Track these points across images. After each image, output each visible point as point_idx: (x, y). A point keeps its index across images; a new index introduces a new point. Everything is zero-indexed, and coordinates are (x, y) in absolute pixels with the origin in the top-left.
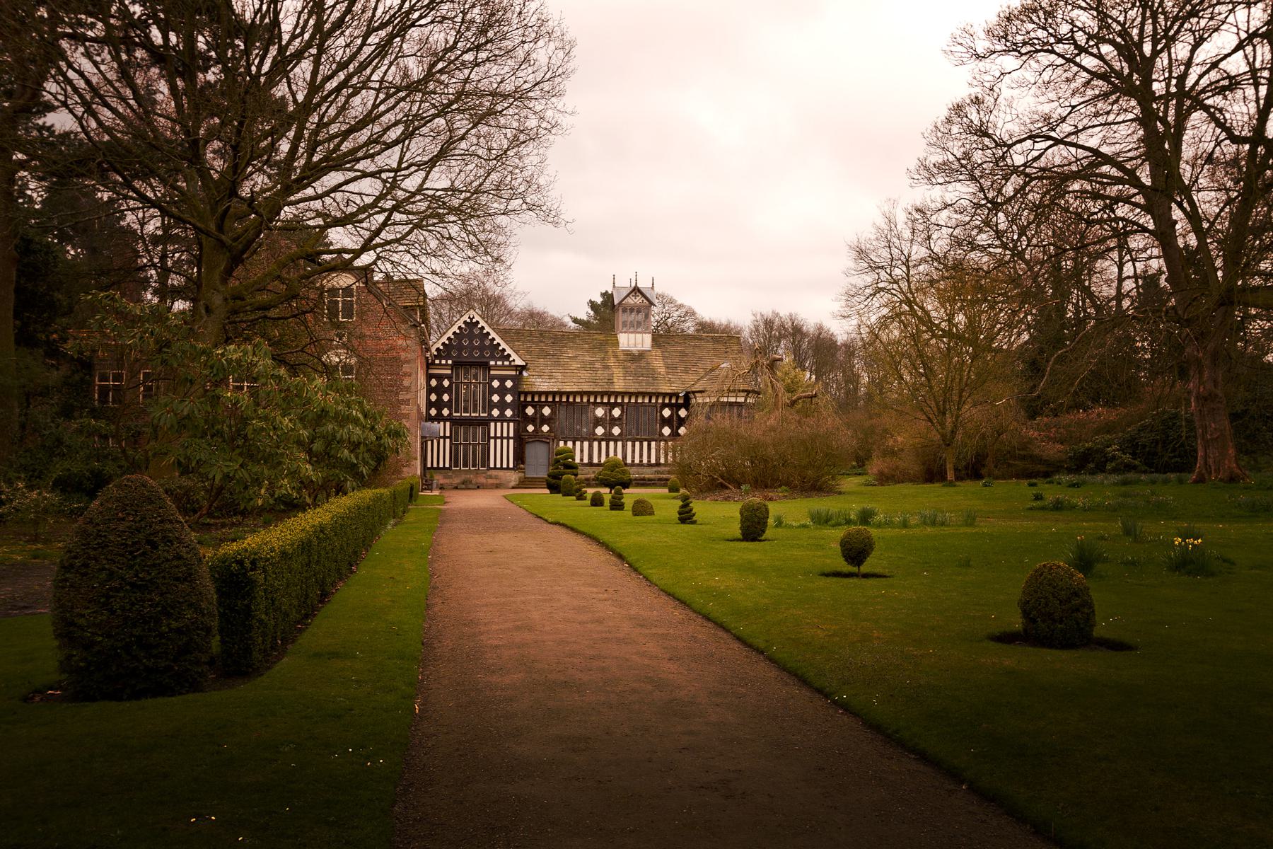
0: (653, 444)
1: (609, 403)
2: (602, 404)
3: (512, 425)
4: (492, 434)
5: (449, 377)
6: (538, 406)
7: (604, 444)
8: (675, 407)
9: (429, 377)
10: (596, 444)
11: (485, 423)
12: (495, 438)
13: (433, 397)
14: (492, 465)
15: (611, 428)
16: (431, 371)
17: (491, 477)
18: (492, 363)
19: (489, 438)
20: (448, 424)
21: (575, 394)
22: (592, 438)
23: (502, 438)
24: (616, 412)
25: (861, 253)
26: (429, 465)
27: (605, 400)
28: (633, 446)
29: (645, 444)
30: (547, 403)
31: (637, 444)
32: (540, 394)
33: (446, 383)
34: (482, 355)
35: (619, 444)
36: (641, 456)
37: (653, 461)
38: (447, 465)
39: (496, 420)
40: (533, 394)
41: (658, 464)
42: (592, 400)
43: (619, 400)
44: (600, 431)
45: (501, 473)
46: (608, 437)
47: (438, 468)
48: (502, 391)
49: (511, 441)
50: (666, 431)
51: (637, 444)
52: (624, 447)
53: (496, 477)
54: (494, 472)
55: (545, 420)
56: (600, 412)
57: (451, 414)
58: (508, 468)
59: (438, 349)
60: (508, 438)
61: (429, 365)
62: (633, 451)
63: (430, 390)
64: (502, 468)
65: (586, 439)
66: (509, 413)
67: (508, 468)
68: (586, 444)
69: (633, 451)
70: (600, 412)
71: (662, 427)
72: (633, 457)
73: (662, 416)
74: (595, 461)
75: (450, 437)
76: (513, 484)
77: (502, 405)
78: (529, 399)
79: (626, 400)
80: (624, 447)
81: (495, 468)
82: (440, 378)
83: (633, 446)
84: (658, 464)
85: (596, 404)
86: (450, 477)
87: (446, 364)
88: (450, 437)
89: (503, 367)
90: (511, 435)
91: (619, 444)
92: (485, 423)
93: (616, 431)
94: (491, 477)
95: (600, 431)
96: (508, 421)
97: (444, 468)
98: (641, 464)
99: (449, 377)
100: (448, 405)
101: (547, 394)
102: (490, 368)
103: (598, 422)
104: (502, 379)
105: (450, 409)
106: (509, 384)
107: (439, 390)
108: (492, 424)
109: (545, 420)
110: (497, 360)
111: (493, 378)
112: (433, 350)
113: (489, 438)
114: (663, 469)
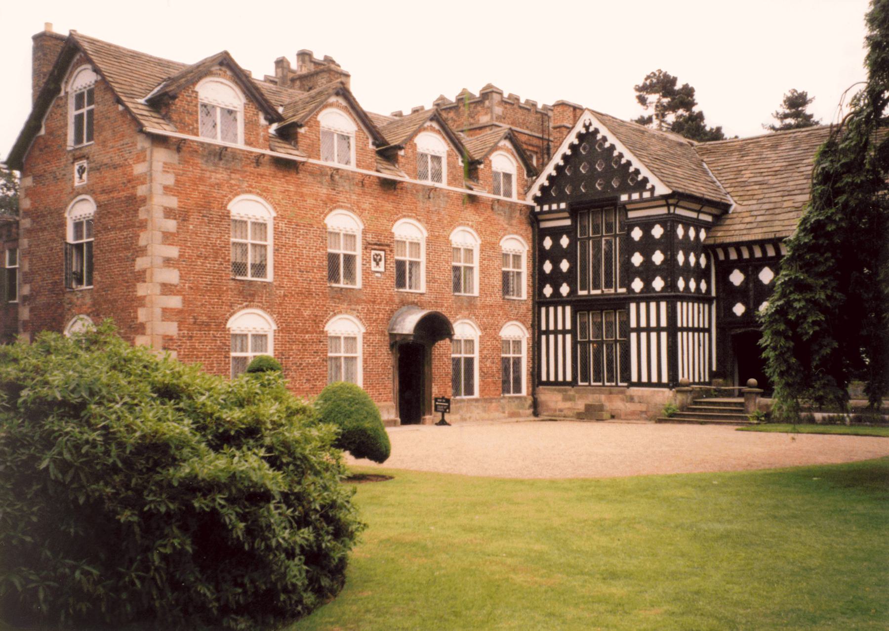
4: (633, 324)
5: (568, 231)
11: (620, 304)
13: (548, 267)
14: (634, 378)
17: (631, 399)
18: (624, 198)
20: (568, 309)
23: (648, 330)
38: (569, 378)
39: (638, 299)
47: (556, 383)
54: (634, 391)
57: (573, 292)
58: (659, 384)
60: (659, 329)
64: (649, 384)
82: (556, 234)
87: (559, 211)
96: (658, 299)
100: (570, 277)
102: (624, 209)
104: (647, 225)
108: (633, 306)
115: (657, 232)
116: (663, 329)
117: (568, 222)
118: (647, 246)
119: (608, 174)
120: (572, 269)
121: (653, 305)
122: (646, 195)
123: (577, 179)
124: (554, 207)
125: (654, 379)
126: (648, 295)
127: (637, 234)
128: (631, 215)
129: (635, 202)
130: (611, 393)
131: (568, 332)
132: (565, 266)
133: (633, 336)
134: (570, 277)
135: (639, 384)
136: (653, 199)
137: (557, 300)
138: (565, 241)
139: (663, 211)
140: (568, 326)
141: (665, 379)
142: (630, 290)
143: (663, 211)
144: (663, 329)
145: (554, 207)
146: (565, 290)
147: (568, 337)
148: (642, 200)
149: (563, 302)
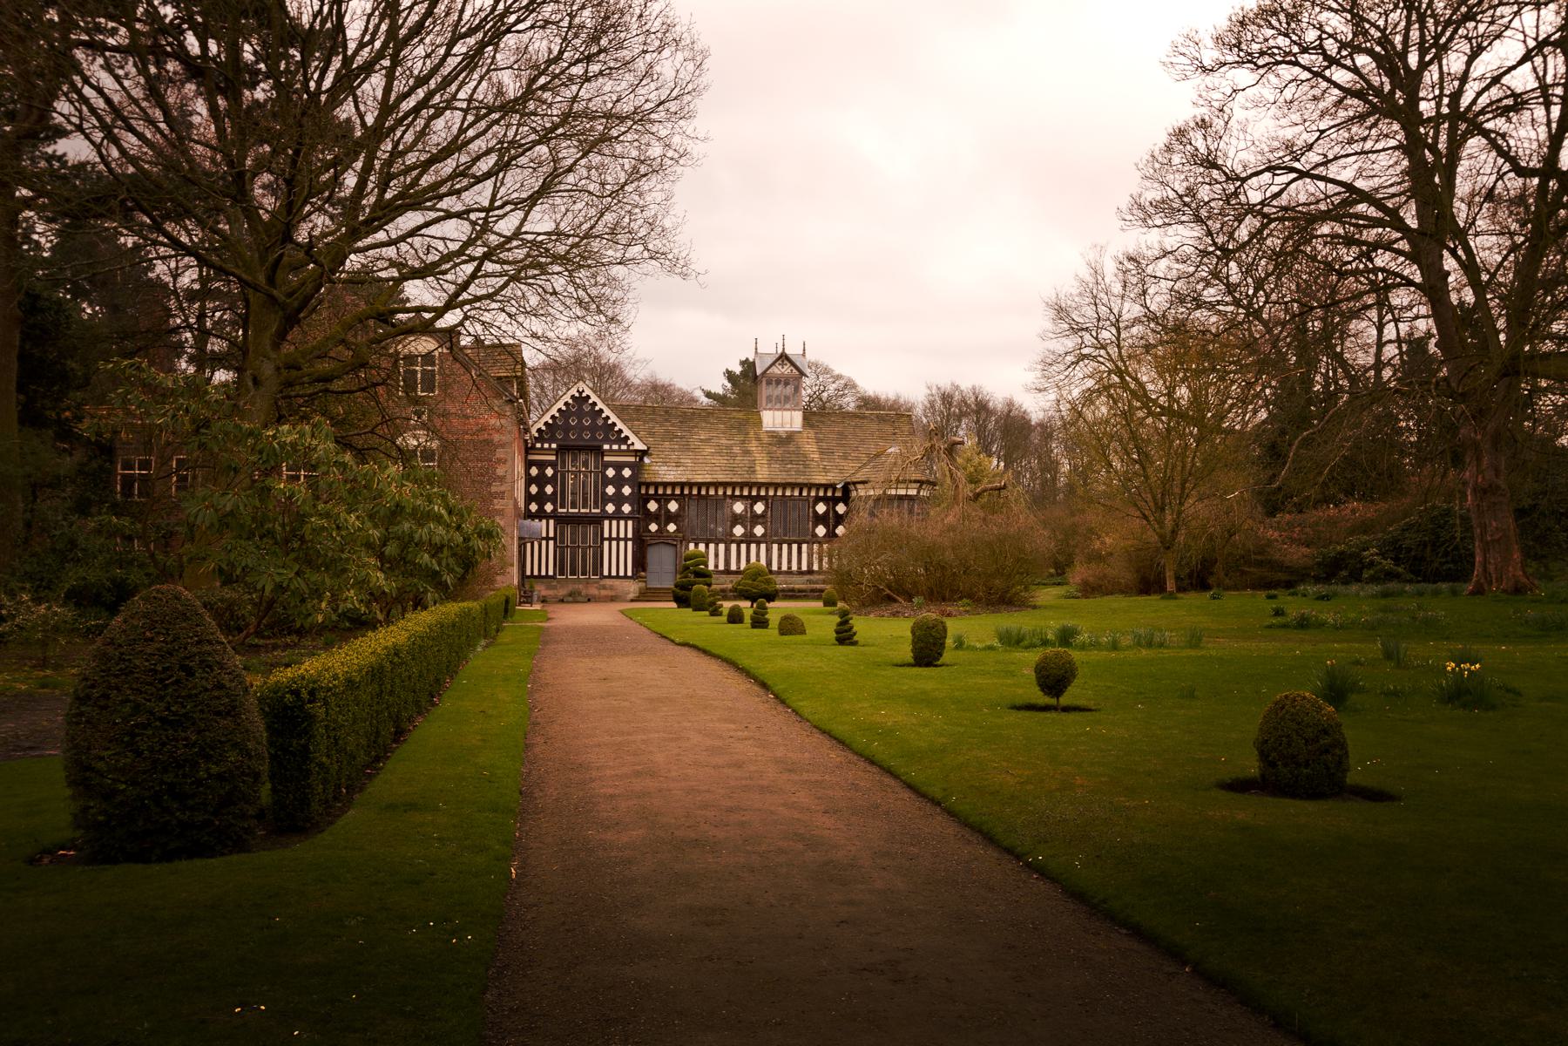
0: (804, 546)
1: (749, 497)
2: (741, 497)
3: (630, 523)
4: (606, 535)
5: (553, 464)
7: (743, 546)
9: (529, 464)
10: (734, 547)
11: (597, 521)
13: (534, 489)
14: (606, 573)
15: (753, 527)
16: (531, 457)
17: (604, 588)
18: (606, 447)
19: (603, 539)
20: (551, 522)
21: (708, 485)
22: (729, 539)
23: (618, 539)
24: (759, 508)
25: (1061, 312)
28: (780, 549)
29: (795, 546)
31: (785, 546)
32: (665, 485)
33: (549, 472)
34: (594, 438)
35: (763, 546)
36: (790, 561)
37: (804, 568)
39: (610, 518)
40: (656, 485)
41: (810, 572)
42: (729, 492)
44: (739, 531)
45: (617, 582)
46: (749, 539)
47: (540, 576)
48: (619, 482)
49: (630, 544)
50: (821, 531)
51: (785, 546)
52: (769, 550)
53: (611, 588)
54: (608, 582)
55: (671, 518)
56: (739, 507)
57: (555, 510)
59: (539, 430)
61: (529, 450)
62: (780, 556)
63: (530, 480)
64: (618, 576)
65: (721, 541)
66: (626, 508)
67: (626, 577)
68: (722, 547)
69: (780, 556)
70: (739, 507)
71: (815, 526)
72: (780, 563)
73: (815, 512)
74: (733, 567)
75: (554, 539)
76: (631, 596)
77: (619, 499)
79: (771, 493)
80: (769, 550)
82: (542, 465)
83: (780, 549)
84: (810, 572)
85: (734, 498)
86: (554, 588)
88: (554, 539)
89: (620, 452)
90: (630, 535)
91: (763, 546)
92: (597, 521)
93: (759, 531)
94: (604, 588)
95: (739, 531)
96: (626, 518)
98: (789, 572)
99: (553, 464)
100: (552, 499)
101: (673, 485)
102: (603, 453)
103: (736, 519)
104: (619, 467)
105: (554, 504)
106: (627, 473)
107: (541, 480)
108: (606, 523)
111: (607, 465)
112: (534, 431)
113: (603, 539)
115: (627, 473)
118: (619, 482)
119: (593, 428)
120: (554, 493)
123: (567, 429)
126: (619, 515)
127: (611, 473)
132: (549, 489)
133: (606, 543)
134: (552, 499)
135: (610, 576)
137: (541, 515)
139: (632, 459)
142: (603, 510)
143: (632, 459)
146: (549, 507)
147: (551, 543)
149: (547, 517)
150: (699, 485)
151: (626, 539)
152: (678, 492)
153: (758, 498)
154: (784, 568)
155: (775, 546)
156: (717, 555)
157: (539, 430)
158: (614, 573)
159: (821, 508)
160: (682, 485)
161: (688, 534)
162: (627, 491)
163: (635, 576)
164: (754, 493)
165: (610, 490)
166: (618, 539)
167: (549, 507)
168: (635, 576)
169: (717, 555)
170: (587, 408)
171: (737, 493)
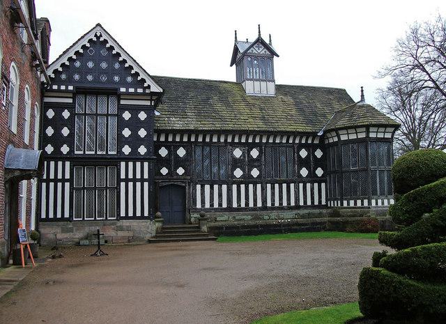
0: (292, 186)
1: (247, 143)
2: (240, 145)
3: (146, 164)
4: (123, 176)
5: (71, 107)
6: (173, 147)
7: (243, 187)
8: (311, 148)
9: (45, 107)
10: (235, 187)
11: (113, 162)
12: (127, 180)
13: (50, 131)
14: (123, 214)
15: (250, 170)
16: (47, 100)
17: (121, 228)
18: (123, 90)
19: (119, 180)
20: (68, 164)
21: (212, 133)
22: (230, 180)
23: (134, 180)
24: (255, 153)
25: (415, 32)
26: (43, 216)
27: (243, 140)
28: (273, 188)
29: (284, 186)
30: (181, 144)
31: (277, 186)
32: (175, 132)
33: (66, 114)
34: (111, 81)
35: (259, 186)
36: (281, 198)
37: (293, 204)
38: (67, 215)
39: (127, 159)
40: (167, 132)
41: (297, 207)
42: (229, 140)
43: (257, 141)
44: (238, 173)
45: (134, 223)
46: (247, 179)
47: (55, 219)
48: (135, 124)
49: (146, 184)
50: (304, 172)
51: (277, 186)
52: (264, 190)
53: (128, 229)
54: (125, 223)
55: (180, 162)
56: (238, 153)
57: (71, 151)
58: (142, 217)
59: (56, 72)
60: (142, 180)
61: (44, 90)
62: (273, 194)
63: (45, 122)
64: (135, 217)
65: (224, 183)
66: (142, 150)
67: (142, 217)
68: (224, 187)
69: (273, 194)
70: (238, 153)
71: (300, 169)
72: (273, 200)
73: (299, 157)
74: (235, 205)
75: (71, 180)
76: (148, 237)
77: (135, 141)
78: (162, 139)
79: (264, 141)
80: (264, 190)
81: (127, 217)
82: (59, 108)
83: (273, 188)
84: (297, 207)
85: (234, 145)
86: (71, 230)
87: (67, 91)
88: (71, 180)
89: (135, 96)
90: (146, 176)
91: (259, 186)
92: (113, 162)
93: (255, 173)
94: (121, 228)
95: (238, 173)
96: (142, 159)
97: (63, 218)
98: (281, 208)
99: (71, 107)
100: (69, 141)
101: (182, 132)
102: (119, 96)
103: (236, 163)
104: (135, 110)
105: (71, 145)
106: (142, 116)
107: (58, 123)
108: (123, 164)
109: (180, 162)
110: (128, 86)
111: (122, 109)
112: (50, 73)
113: (119, 180)
114: (302, 212)
116: (146, 180)
117: (70, 101)
119: (110, 72)
120: (71, 135)
121: (138, 164)
122: (140, 90)
123: (84, 71)
124: (63, 88)
125: (138, 214)
126: (134, 157)
128: (122, 102)
129: (131, 94)
130: (104, 225)
131: (67, 180)
133: (123, 184)
135: (127, 217)
136: (144, 94)
137: (57, 156)
138: (66, 114)
140: (67, 176)
141: (146, 214)
144: (146, 180)
145: (63, 88)
146: (65, 149)
147: (67, 185)
148: (136, 94)
150: (205, 133)
151: (142, 180)
152: (185, 139)
153: (254, 145)
154: (277, 204)
155: (269, 186)
156: (220, 195)
157: (56, 72)
158: (131, 214)
159: (303, 153)
160: (189, 132)
161: (195, 177)
162: (142, 133)
163: (152, 216)
164: (250, 140)
165: (127, 133)
166: (134, 180)
167: (65, 149)
168: (152, 216)
169: (220, 195)
170: (104, 53)
171: (236, 140)
